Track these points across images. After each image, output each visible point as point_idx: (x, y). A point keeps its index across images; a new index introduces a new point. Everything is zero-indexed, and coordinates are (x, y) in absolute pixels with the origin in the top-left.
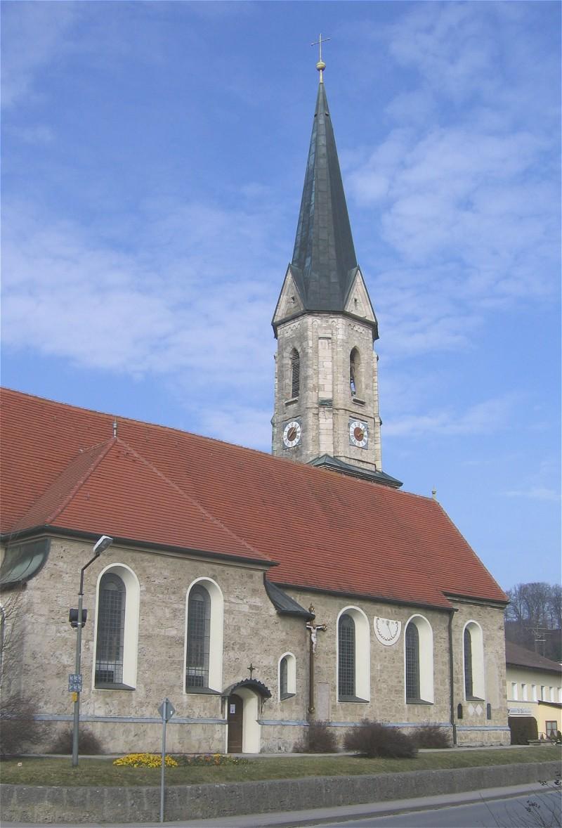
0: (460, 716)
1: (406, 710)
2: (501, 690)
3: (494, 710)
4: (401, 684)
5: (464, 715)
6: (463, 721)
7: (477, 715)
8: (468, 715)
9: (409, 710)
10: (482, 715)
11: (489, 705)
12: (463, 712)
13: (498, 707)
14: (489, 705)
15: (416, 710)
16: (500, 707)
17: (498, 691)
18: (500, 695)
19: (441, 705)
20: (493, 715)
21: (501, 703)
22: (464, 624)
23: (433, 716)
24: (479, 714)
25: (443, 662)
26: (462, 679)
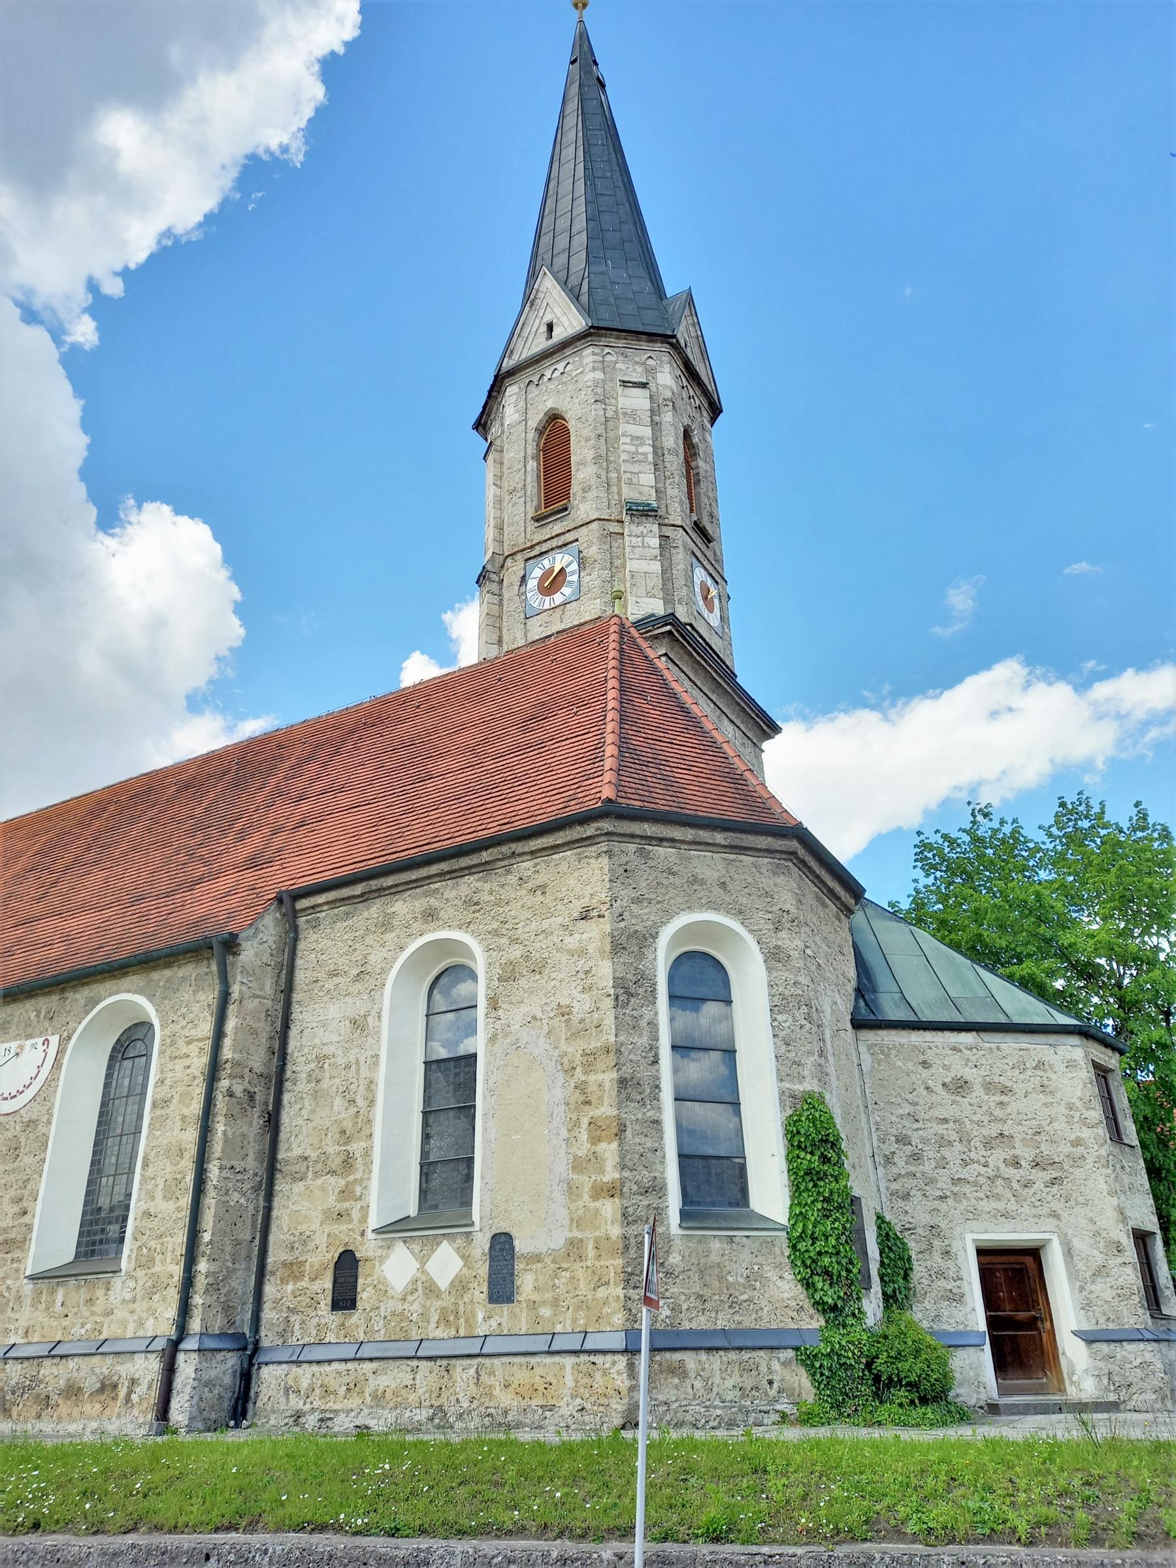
0: (344, 1298)
1: (28, 1301)
2: (578, 1166)
3: (536, 1258)
4: (26, 1219)
5: (365, 1296)
6: (355, 1318)
7: (431, 1290)
8: (383, 1291)
9: (36, 1300)
10: (460, 1286)
11: (502, 1245)
12: (360, 1281)
13: (558, 1241)
14: (502, 1245)
15: (59, 1298)
16: (571, 1243)
17: (562, 1168)
18: (572, 1190)
19: (157, 1268)
20: (526, 1282)
21: (577, 1223)
22: (395, 959)
23: (120, 1314)
24: (443, 1283)
25: (184, 1117)
26: (367, 1153)
